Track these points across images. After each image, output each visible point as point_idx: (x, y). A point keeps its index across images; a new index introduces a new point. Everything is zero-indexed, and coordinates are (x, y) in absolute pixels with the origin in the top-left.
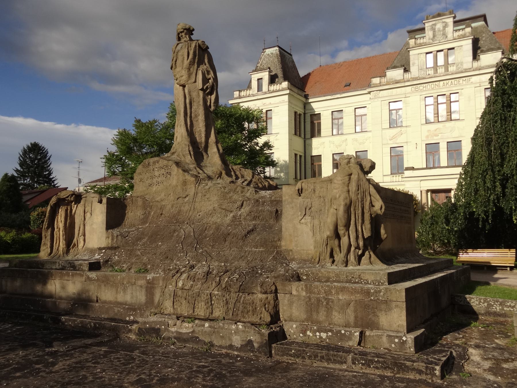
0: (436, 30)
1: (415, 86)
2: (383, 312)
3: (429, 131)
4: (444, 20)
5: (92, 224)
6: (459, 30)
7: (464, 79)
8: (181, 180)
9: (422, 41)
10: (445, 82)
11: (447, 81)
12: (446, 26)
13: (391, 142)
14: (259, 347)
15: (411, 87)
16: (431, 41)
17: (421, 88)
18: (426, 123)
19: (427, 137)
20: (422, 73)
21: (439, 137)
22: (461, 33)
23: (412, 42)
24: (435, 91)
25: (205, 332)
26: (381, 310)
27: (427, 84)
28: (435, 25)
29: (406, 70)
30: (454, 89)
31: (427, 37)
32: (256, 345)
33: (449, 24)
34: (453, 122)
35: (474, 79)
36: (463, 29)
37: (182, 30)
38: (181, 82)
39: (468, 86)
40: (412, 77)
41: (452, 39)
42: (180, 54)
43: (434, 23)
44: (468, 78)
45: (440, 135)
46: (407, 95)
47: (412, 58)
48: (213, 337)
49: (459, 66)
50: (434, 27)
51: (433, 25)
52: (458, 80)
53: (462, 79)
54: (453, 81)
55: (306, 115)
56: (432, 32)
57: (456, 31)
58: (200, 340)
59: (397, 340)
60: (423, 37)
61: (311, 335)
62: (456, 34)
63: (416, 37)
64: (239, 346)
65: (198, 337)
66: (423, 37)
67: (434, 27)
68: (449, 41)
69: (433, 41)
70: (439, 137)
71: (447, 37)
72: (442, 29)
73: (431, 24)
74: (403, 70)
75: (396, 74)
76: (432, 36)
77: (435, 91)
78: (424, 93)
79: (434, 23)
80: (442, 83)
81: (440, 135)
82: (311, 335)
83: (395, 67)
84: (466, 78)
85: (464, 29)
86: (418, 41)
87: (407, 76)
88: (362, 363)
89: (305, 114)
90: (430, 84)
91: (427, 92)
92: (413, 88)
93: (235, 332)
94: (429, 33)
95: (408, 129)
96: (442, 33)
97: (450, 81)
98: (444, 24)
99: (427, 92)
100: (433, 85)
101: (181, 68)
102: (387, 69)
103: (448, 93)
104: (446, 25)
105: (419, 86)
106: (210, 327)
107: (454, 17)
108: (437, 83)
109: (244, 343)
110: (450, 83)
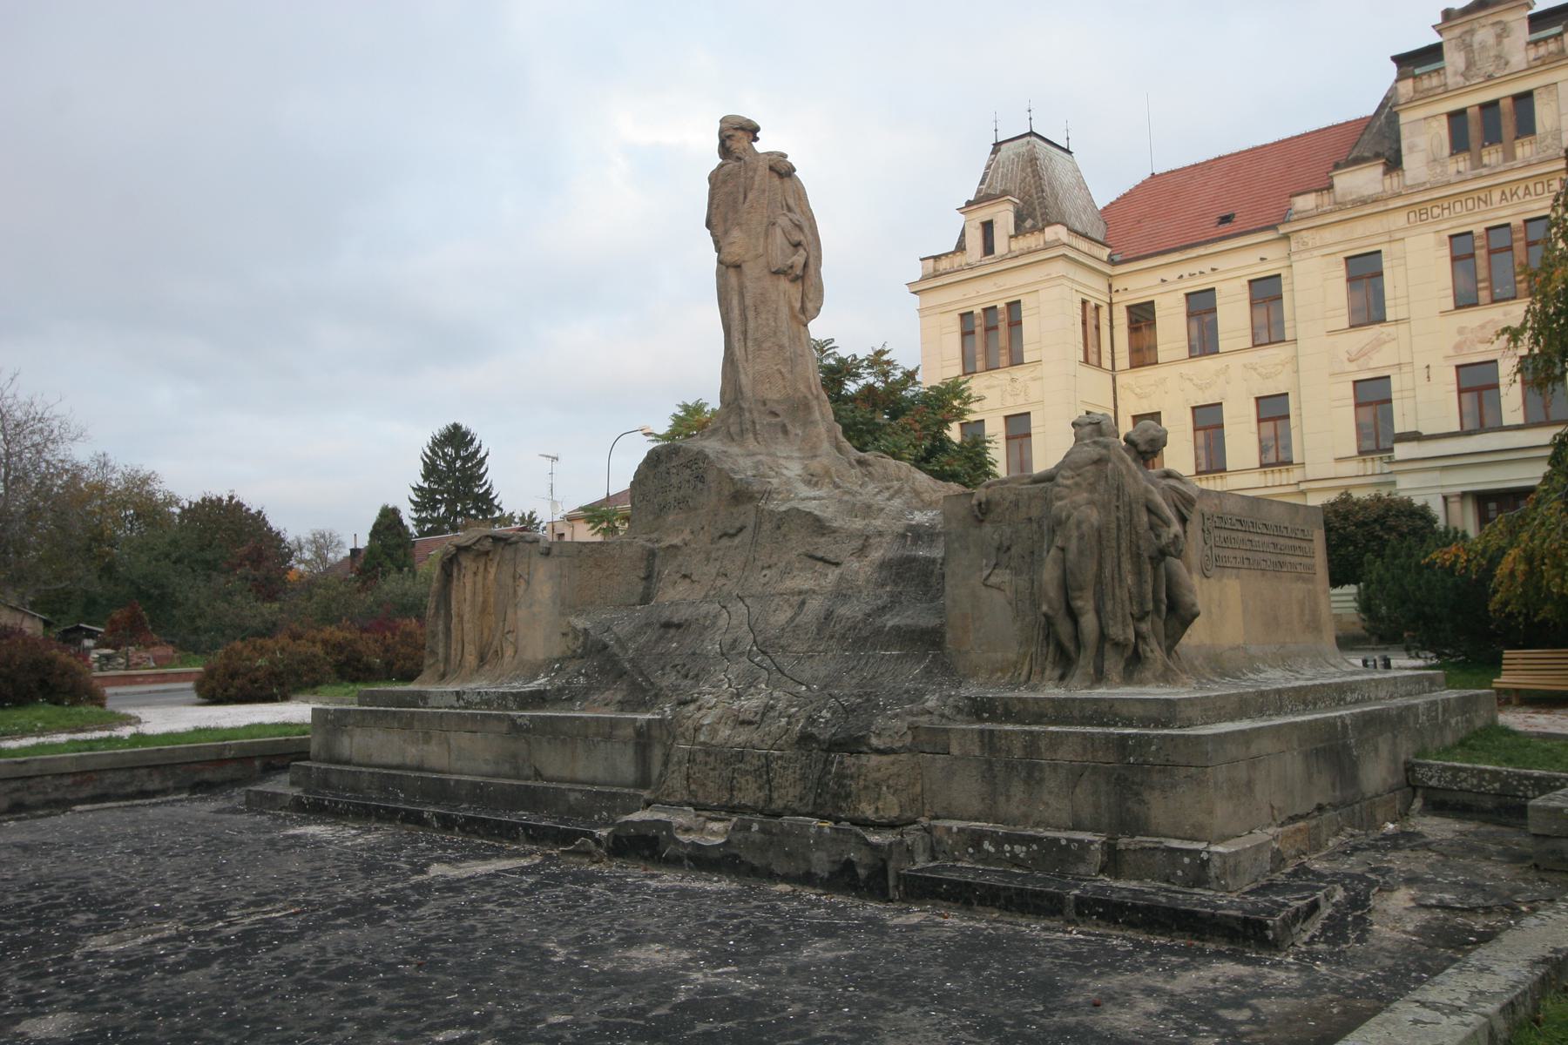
0: (1476, 46)
2: (1157, 793)
6: (1545, 40)
9: (1435, 81)
12: (1503, 32)
13: (1353, 367)
14: (869, 877)
15: (1404, 213)
16: (1460, 79)
17: (1436, 211)
19: (1458, 347)
22: (1552, 46)
24: (1479, 218)
25: (753, 842)
26: (1152, 788)
28: (1472, 32)
29: (1394, 164)
31: (1450, 70)
32: (862, 872)
41: (1524, 66)
43: (1466, 28)
46: (1398, 236)
47: (1405, 132)
48: (771, 854)
50: (1468, 38)
55: (1115, 308)
57: (1536, 43)
58: (742, 862)
59: (1187, 860)
61: (992, 849)
63: (1417, 71)
64: (826, 875)
65: (736, 856)
67: (1468, 38)
71: (1507, 63)
72: (1491, 41)
74: (1380, 169)
75: (1363, 180)
76: (1461, 65)
77: (1479, 218)
79: (1466, 28)
82: (992, 849)
83: (1358, 161)
86: (1426, 83)
87: (1393, 183)
88: (1097, 913)
89: (1111, 305)
91: (1454, 223)
93: (816, 843)
95: (1402, 327)
98: (1498, 29)
99: (1454, 223)
100: (1470, 203)
102: (1337, 166)
104: (1504, 30)
106: (762, 830)
109: (836, 868)
110: (1521, 193)
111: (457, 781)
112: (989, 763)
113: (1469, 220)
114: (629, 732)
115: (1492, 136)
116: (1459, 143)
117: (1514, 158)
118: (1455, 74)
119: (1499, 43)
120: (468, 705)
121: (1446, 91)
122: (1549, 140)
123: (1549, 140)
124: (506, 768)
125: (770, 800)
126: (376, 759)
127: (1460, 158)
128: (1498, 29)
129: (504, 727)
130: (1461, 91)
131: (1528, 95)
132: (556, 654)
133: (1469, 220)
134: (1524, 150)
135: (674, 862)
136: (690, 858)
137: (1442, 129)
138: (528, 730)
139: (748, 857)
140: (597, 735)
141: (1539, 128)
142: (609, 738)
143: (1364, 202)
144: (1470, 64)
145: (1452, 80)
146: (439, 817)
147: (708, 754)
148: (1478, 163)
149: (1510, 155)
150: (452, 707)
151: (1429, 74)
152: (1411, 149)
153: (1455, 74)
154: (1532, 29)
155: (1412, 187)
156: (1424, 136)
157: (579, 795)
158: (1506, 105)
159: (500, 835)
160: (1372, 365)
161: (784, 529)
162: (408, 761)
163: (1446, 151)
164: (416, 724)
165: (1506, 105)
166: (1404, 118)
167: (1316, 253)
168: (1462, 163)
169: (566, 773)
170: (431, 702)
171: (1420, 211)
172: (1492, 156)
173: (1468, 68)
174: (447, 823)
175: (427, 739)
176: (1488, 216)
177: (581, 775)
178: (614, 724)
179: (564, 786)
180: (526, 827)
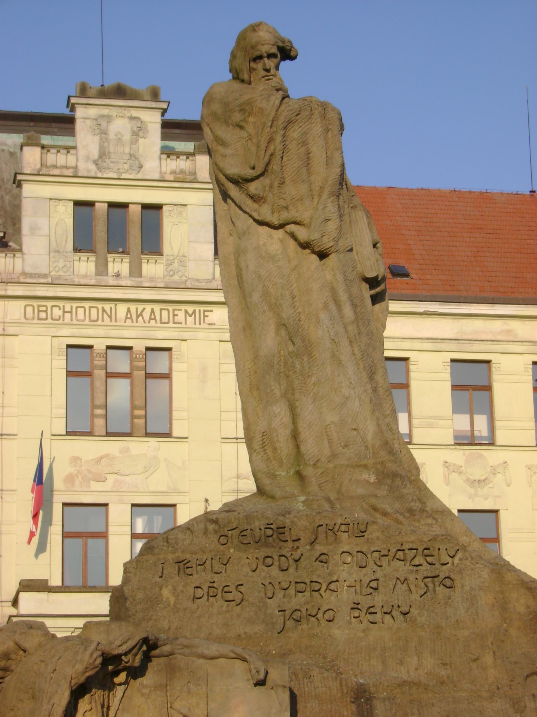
0: (112, 136)
1: (35, 303)
3: (75, 460)
4: (135, 113)
6: (178, 155)
7: (190, 309)
8: (522, 609)
9: (61, 159)
10: (133, 307)
11: (140, 307)
12: (140, 131)
15: (22, 303)
16: (93, 167)
17: (57, 312)
18: (68, 433)
20: (61, 264)
21: (108, 485)
22: (182, 164)
23: (31, 156)
24: (101, 332)
27: (75, 304)
28: (109, 119)
30: (160, 334)
31: (82, 152)
33: (150, 127)
34: (153, 442)
36: (189, 155)
37: (274, 50)
38: (325, 239)
39: (201, 335)
40: (28, 270)
41: (157, 176)
42: (295, 133)
43: (105, 111)
44: (202, 308)
45: (111, 478)
46: (11, 330)
49: (176, 265)
50: (104, 124)
51: (103, 116)
52: (171, 307)
53: (183, 307)
54: (157, 308)
56: (97, 138)
60: (68, 149)
62: (173, 165)
66: (68, 149)
68: (146, 183)
69: (99, 168)
70: (108, 485)
71: (141, 167)
72: (127, 137)
73: (93, 112)
76: (95, 154)
77: (101, 332)
78: (65, 332)
80: (122, 309)
81: (111, 478)
84: (197, 308)
85: (194, 155)
86: (51, 158)
90: (87, 305)
91: (75, 331)
92: (29, 310)
94: (85, 138)
96: (127, 150)
97: (149, 308)
98: (135, 124)
99: (75, 331)
100: (94, 311)
101: (303, 189)
103: (139, 346)
104: (140, 128)
105: (49, 304)
107: (164, 112)
108: (107, 306)
110: (147, 315)
113: (91, 332)
115: (117, 243)
116: (83, 243)
117: (140, 275)
118: (88, 158)
119: (135, 142)
121: (75, 175)
127: (84, 256)
128: (135, 124)
130: (91, 180)
131: (158, 207)
133: (91, 332)
134: (152, 268)
137: (65, 215)
141: (166, 249)
144: (103, 154)
145: (86, 167)
148: (102, 269)
149: (136, 271)
151: (59, 149)
152: (34, 229)
153: (88, 158)
154: (164, 137)
155: (31, 275)
158: (135, 211)
165: (135, 211)
166: (28, 190)
168: (86, 265)
172: (119, 265)
173: (100, 157)
176: (114, 332)
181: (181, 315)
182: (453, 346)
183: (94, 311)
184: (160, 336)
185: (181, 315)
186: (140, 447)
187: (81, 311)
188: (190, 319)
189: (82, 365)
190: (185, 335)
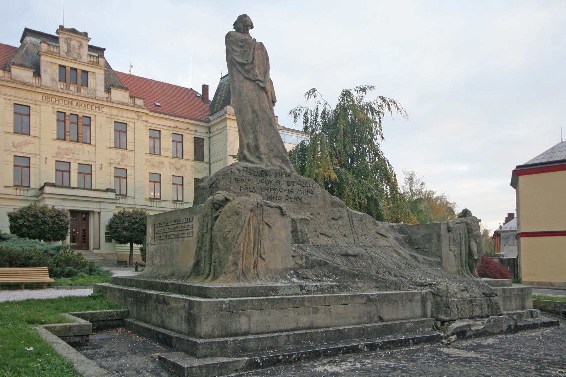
5: (273, 240)
17: (53, 100)
24: (68, 109)
30: (87, 112)
35: (105, 109)
39: (100, 114)
46: (38, 103)
53: (95, 105)
91: (60, 107)
92: (44, 98)
99: (60, 107)
110: (83, 106)
111: (349, 329)
112: (504, 297)
113: (65, 108)
114: (419, 297)
120: (309, 292)
122: (92, 91)
123: (92, 91)
124: (365, 319)
125: (482, 312)
126: (273, 327)
129: (364, 300)
132: (289, 266)
133: (65, 108)
135: (470, 337)
136: (474, 335)
138: (376, 301)
139: (490, 330)
140: (406, 300)
142: (411, 300)
143: (25, 84)
146: (367, 346)
147: (464, 301)
150: (296, 294)
156: (50, 70)
157: (410, 324)
159: (401, 346)
160: (24, 151)
161: (364, 221)
162: (301, 325)
163: (58, 79)
164: (307, 304)
167: (104, 115)
169: (394, 317)
170: (280, 292)
171: (48, 97)
174: (372, 347)
175: (316, 310)
177: (400, 317)
178: (414, 294)
179: (404, 321)
180: (413, 339)
181: (94, 108)
182: (173, 129)
183: (66, 102)
184: (88, 113)
185: (94, 108)
186: (79, 146)
187: (61, 101)
188: (97, 109)
189: (62, 117)
190: (95, 114)
